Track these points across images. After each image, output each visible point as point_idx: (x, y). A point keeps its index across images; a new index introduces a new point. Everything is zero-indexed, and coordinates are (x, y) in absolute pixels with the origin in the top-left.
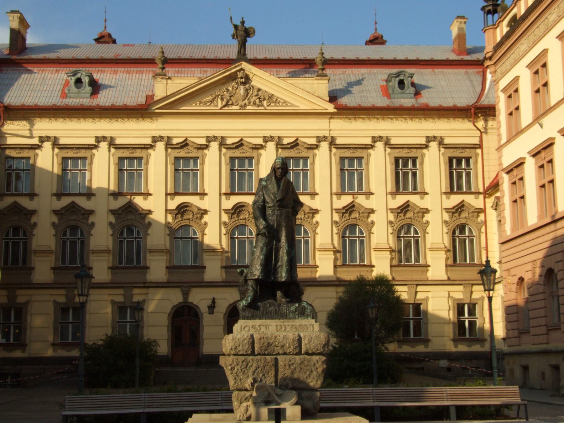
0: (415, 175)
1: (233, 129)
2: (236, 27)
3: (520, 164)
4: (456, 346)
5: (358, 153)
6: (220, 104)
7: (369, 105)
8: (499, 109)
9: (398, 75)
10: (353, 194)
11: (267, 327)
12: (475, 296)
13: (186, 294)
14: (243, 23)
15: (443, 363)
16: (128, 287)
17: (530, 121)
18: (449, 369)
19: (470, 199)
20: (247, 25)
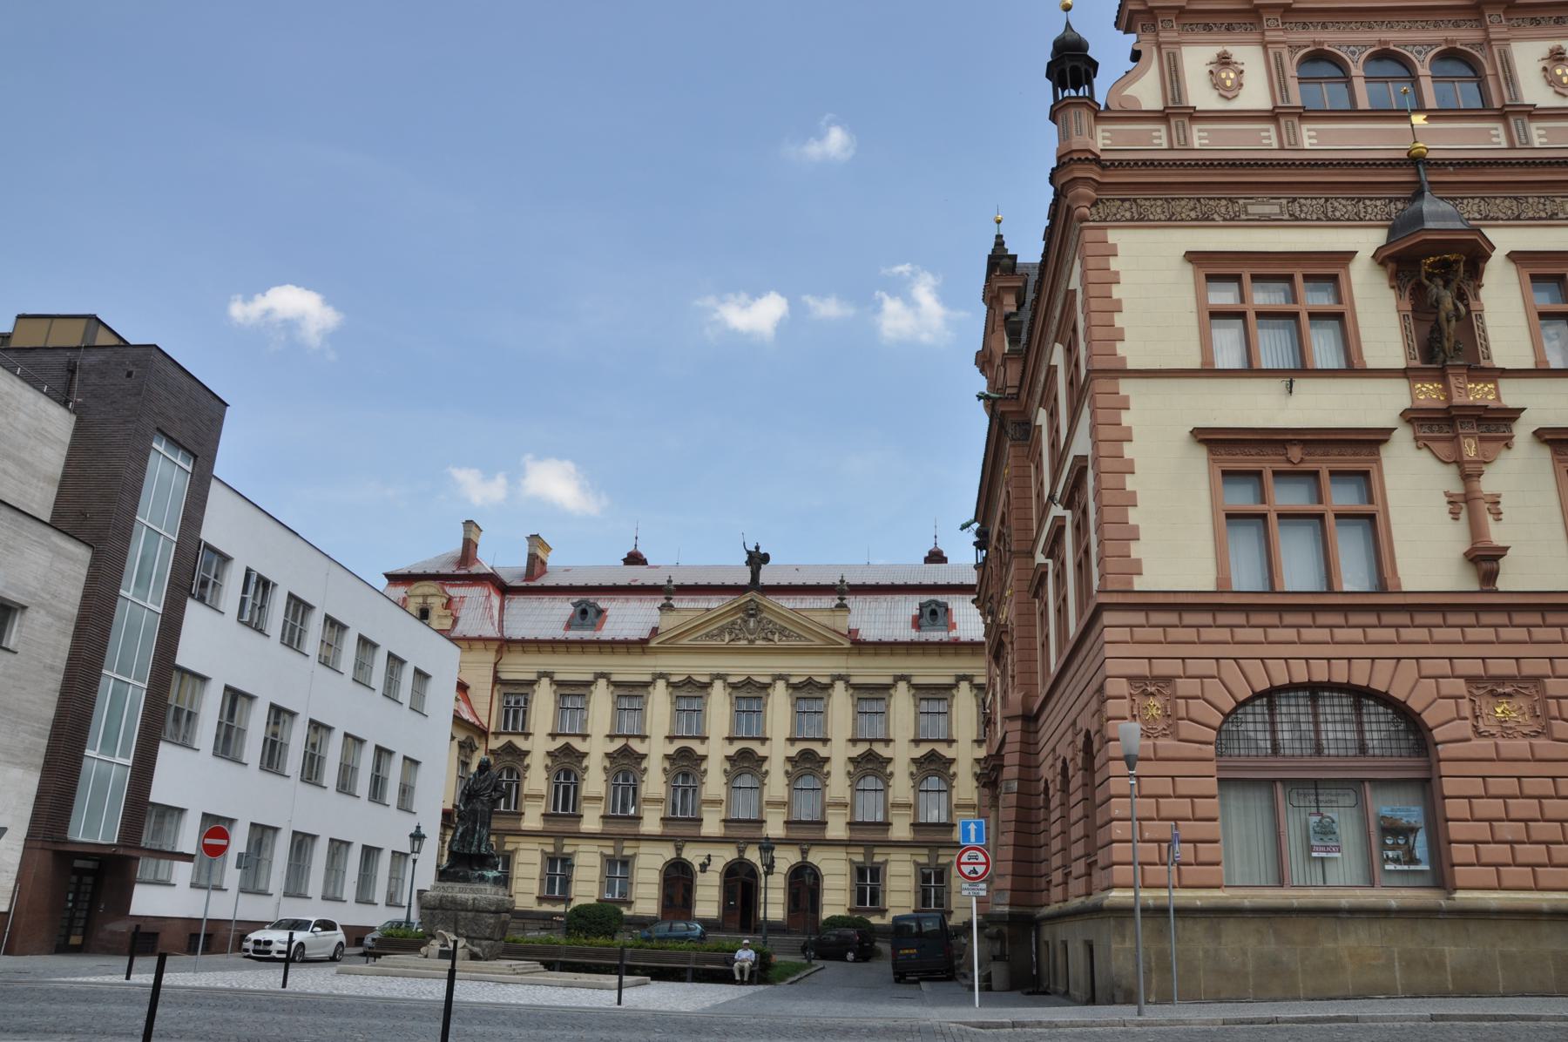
1: (740, 667)
2: (749, 553)
6: (727, 638)
13: (679, 850)
14: (757, 548)
20: (762, 551)
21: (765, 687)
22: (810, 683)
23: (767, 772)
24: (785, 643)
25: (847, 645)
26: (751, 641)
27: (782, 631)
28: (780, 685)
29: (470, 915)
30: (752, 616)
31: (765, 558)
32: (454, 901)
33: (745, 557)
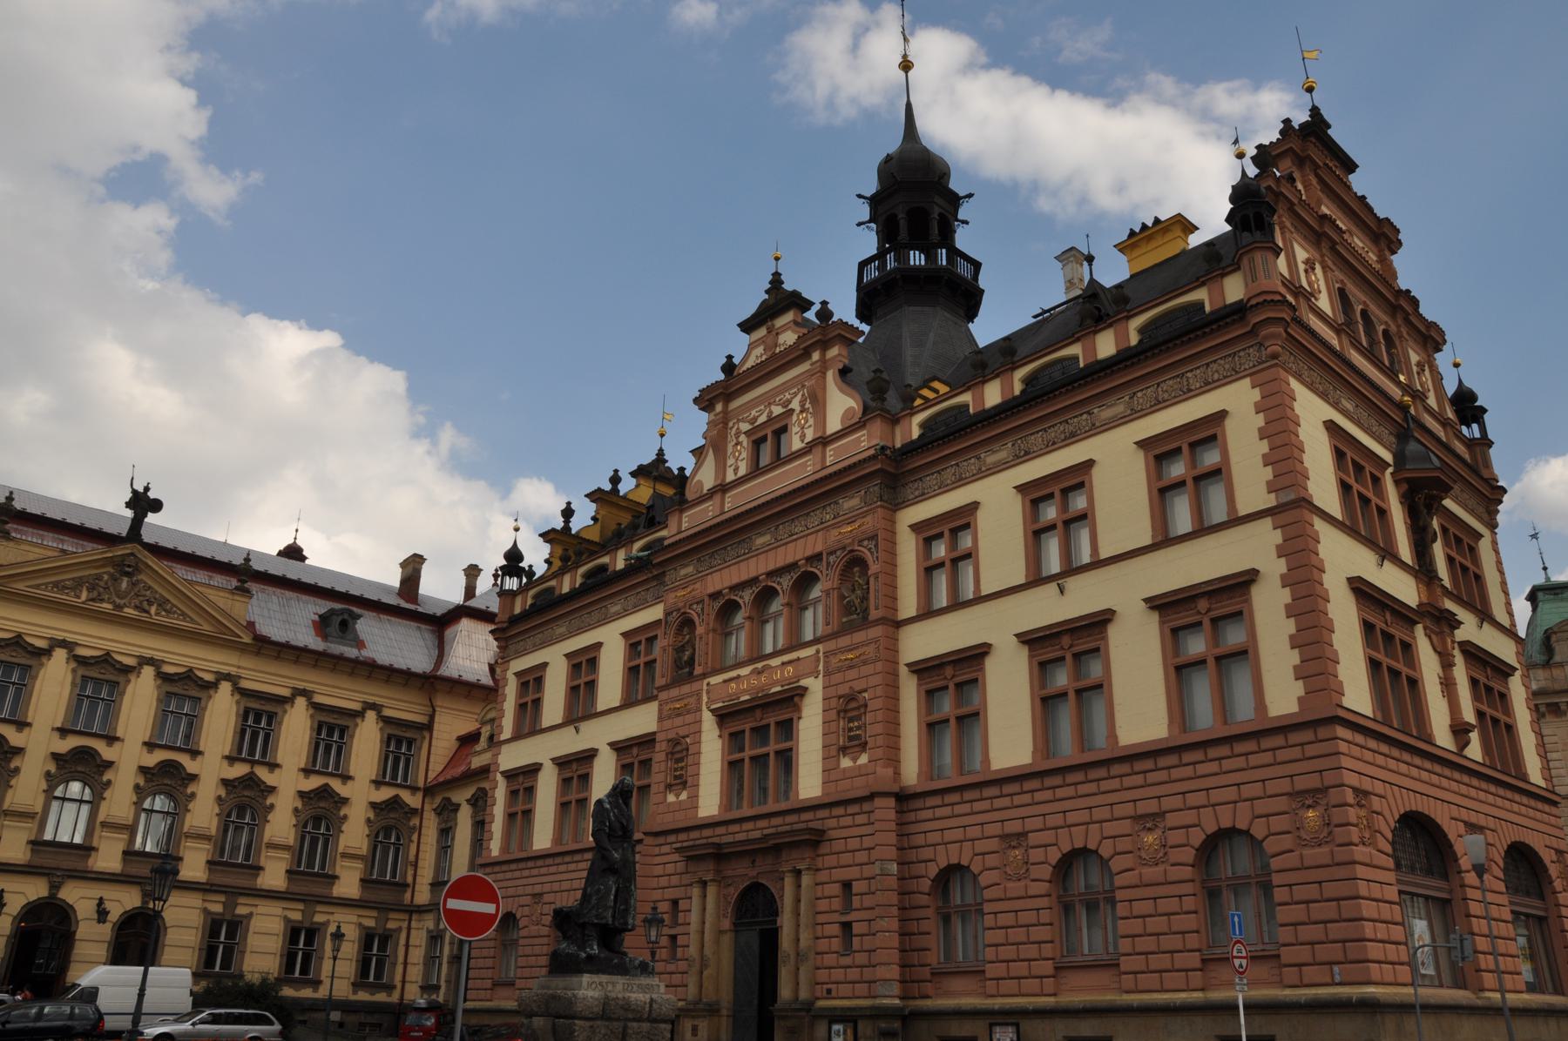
0: (267, 737)
1: (95, 637)
2: (135, 492)
3: (533, 770)
4: (355, 993)
5: (269, 708)
6: (84, 596)
7: (301, 645)
8: (505, 696)
9: (342, 611)
10: (253, 763)
11: (614, 984)
12: (391, 925)
14: (147, 489)
15: (335, 1016)
16: (232, 894)
17: (560, 721)
18: (341, 1025)
19: (406, 796)
20: (151, 495)
21: (127, 670)
22: (189, 677)
23: (109, 782)
24: (163, 619)
25: (247, 639)
26: (119, 607)
27: (163, 604)
28: (148, 671)
29: (646, 1026)
30: (128, 574)
31: (157, 506)
32: (627, 1006)
33: (128, 496)
